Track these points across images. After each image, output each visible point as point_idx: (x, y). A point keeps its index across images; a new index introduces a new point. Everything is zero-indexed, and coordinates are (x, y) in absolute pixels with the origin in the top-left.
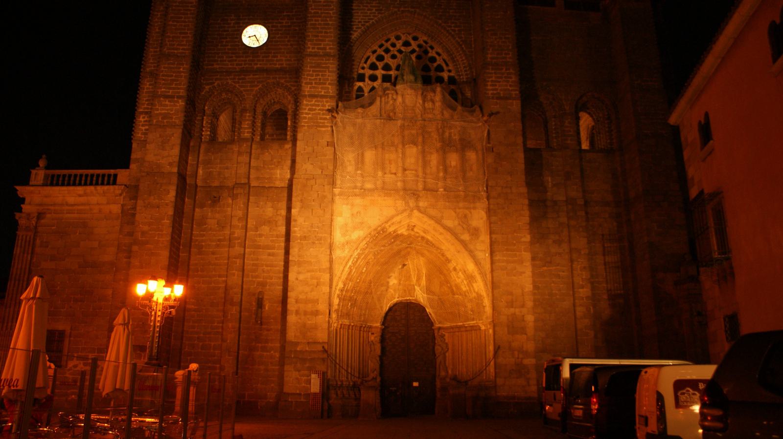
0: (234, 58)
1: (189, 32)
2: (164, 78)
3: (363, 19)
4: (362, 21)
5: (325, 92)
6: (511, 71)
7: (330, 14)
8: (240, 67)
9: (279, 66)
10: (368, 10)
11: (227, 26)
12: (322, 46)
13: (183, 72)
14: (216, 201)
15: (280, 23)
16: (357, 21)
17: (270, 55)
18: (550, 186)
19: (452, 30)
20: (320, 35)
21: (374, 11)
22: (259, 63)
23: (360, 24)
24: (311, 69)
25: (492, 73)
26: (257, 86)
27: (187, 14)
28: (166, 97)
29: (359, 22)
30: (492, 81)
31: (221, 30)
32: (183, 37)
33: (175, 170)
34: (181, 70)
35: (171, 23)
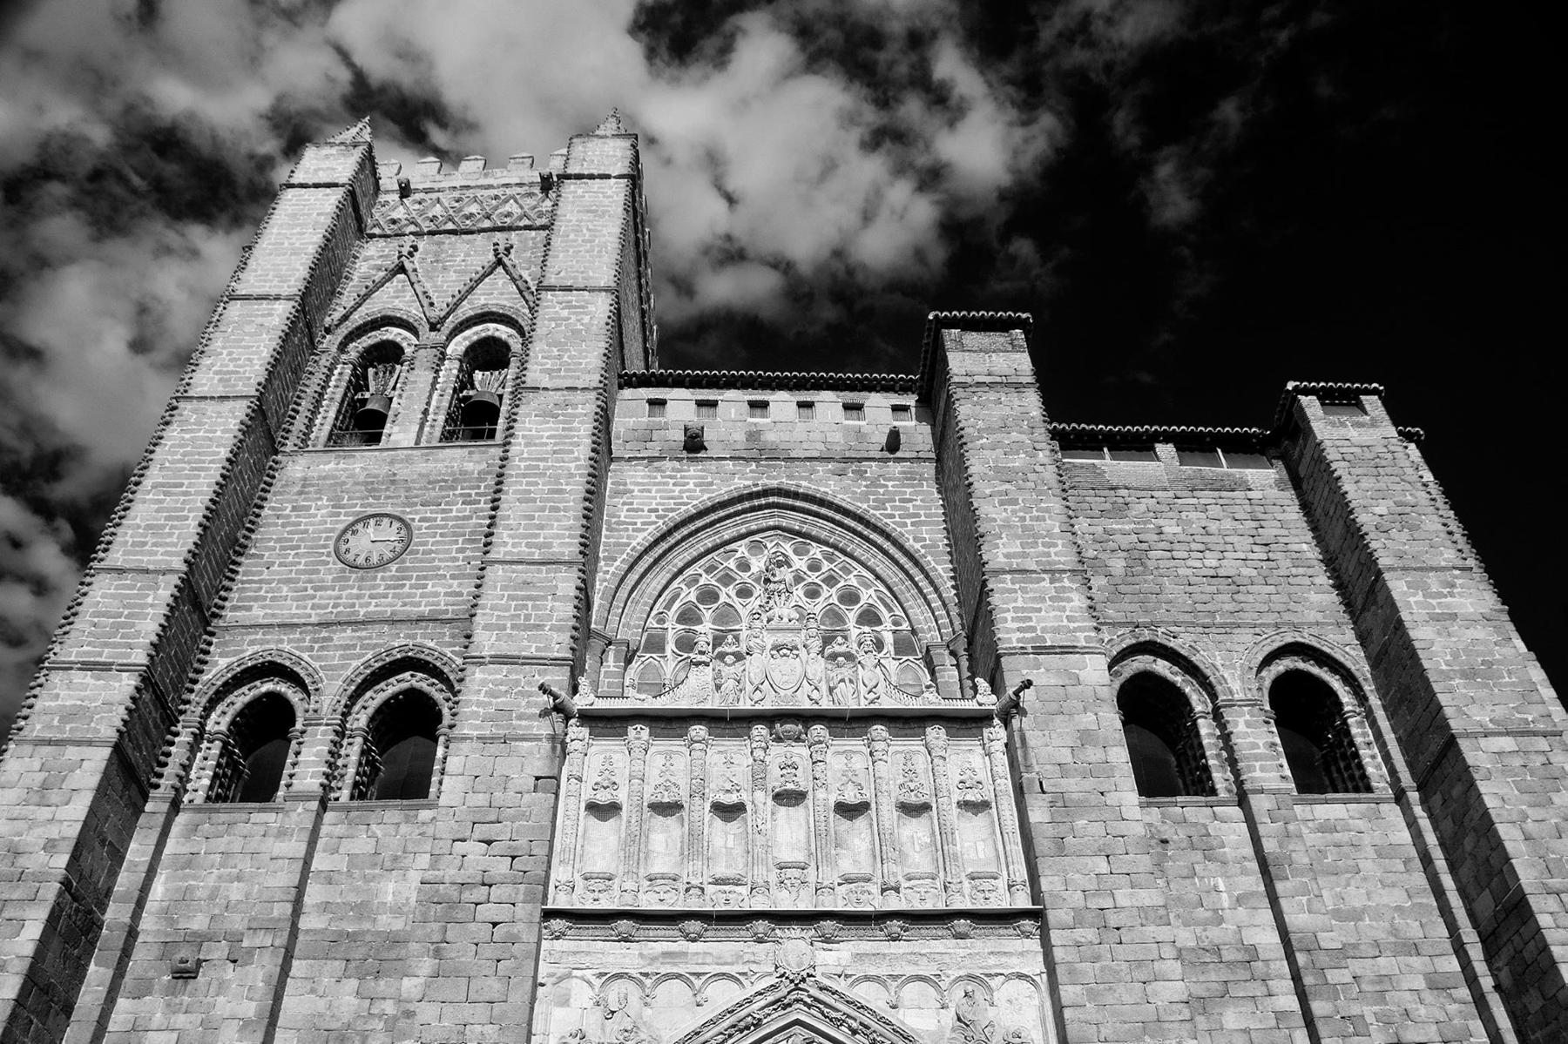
0: (310, 592)
1: (191, 515)
2: (96, 620)
3: (663, 504)
4: (660, 507)
5: (538, 649)
6: (1067, 583)
7: (568, 469)
8: (322, 612)
9: (428, 608)
10: (674, 485)
11: (304, 520)
12: (542, 540)
13: (152, 605)
14: (185, 974)
15: (444, 511)
16: (646, 508)
17: (408, 583)
18: (1226, 905)
19: (893, 523)
20: (537, 514)
21: (691, 486)
22: (374, 601)
23: (653, 514)
24: (506, 594)
25: (1015, 591)
26: (360, 656)
27: (199, 477)
28: (87, 666)
29: (650, 511)
30: (1016, 609)
31: (288, 529)
32: (172, 527)
33: (61, 861)
34: (150, 600)
35: (151, 496)
